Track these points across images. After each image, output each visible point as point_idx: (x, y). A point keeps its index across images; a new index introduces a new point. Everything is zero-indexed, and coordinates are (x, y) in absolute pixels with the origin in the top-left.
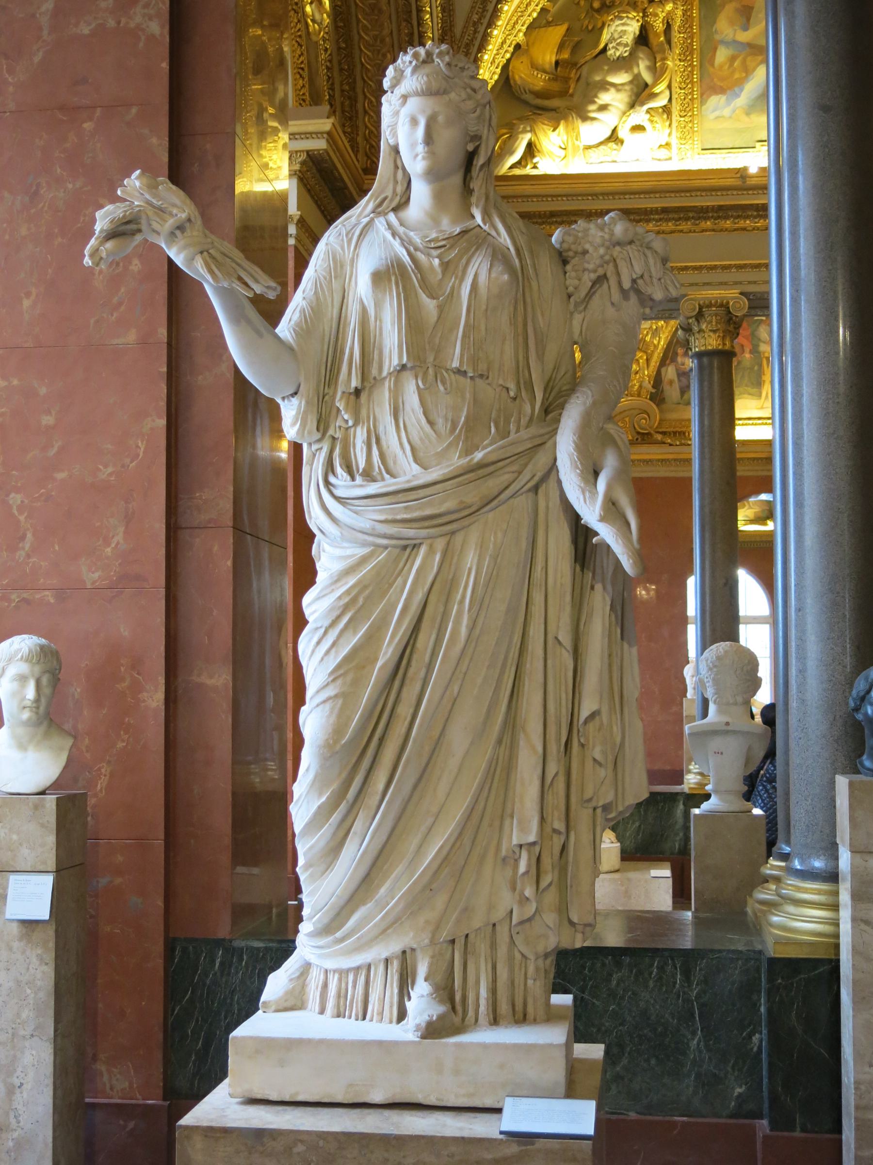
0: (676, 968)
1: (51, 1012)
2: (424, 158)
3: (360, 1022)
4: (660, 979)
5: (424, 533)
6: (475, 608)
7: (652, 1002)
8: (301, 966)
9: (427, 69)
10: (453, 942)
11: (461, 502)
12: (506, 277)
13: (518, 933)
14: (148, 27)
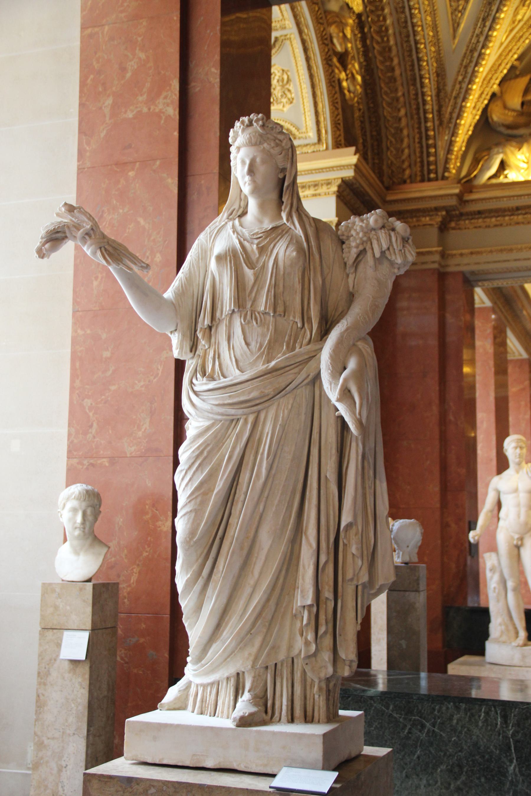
0: (497, 714)
1: (86, 719)
2: (249, 184)
3: (212, 718)
4: (486, 721)
5: (240, 412)
6: (271, 457)
7: (481, 736)
8: (186, 684)
9: (250, 130)
10: (267, 668)
11: (262, 392)
12: (294, 254)
13: (307, 664)
14: (166, 110)
